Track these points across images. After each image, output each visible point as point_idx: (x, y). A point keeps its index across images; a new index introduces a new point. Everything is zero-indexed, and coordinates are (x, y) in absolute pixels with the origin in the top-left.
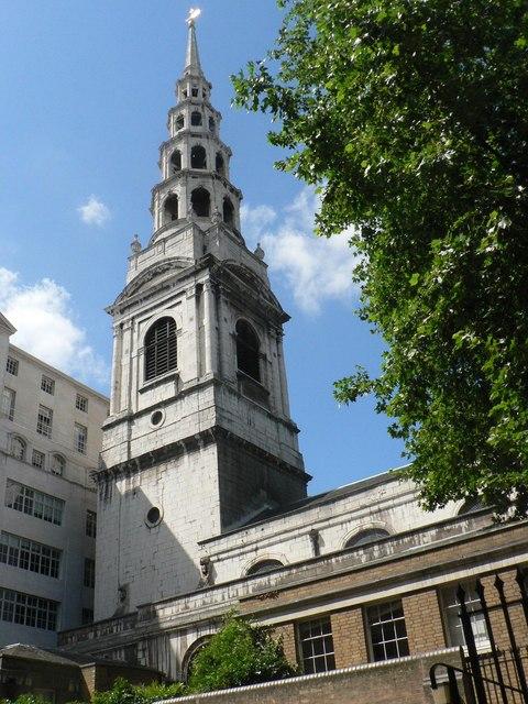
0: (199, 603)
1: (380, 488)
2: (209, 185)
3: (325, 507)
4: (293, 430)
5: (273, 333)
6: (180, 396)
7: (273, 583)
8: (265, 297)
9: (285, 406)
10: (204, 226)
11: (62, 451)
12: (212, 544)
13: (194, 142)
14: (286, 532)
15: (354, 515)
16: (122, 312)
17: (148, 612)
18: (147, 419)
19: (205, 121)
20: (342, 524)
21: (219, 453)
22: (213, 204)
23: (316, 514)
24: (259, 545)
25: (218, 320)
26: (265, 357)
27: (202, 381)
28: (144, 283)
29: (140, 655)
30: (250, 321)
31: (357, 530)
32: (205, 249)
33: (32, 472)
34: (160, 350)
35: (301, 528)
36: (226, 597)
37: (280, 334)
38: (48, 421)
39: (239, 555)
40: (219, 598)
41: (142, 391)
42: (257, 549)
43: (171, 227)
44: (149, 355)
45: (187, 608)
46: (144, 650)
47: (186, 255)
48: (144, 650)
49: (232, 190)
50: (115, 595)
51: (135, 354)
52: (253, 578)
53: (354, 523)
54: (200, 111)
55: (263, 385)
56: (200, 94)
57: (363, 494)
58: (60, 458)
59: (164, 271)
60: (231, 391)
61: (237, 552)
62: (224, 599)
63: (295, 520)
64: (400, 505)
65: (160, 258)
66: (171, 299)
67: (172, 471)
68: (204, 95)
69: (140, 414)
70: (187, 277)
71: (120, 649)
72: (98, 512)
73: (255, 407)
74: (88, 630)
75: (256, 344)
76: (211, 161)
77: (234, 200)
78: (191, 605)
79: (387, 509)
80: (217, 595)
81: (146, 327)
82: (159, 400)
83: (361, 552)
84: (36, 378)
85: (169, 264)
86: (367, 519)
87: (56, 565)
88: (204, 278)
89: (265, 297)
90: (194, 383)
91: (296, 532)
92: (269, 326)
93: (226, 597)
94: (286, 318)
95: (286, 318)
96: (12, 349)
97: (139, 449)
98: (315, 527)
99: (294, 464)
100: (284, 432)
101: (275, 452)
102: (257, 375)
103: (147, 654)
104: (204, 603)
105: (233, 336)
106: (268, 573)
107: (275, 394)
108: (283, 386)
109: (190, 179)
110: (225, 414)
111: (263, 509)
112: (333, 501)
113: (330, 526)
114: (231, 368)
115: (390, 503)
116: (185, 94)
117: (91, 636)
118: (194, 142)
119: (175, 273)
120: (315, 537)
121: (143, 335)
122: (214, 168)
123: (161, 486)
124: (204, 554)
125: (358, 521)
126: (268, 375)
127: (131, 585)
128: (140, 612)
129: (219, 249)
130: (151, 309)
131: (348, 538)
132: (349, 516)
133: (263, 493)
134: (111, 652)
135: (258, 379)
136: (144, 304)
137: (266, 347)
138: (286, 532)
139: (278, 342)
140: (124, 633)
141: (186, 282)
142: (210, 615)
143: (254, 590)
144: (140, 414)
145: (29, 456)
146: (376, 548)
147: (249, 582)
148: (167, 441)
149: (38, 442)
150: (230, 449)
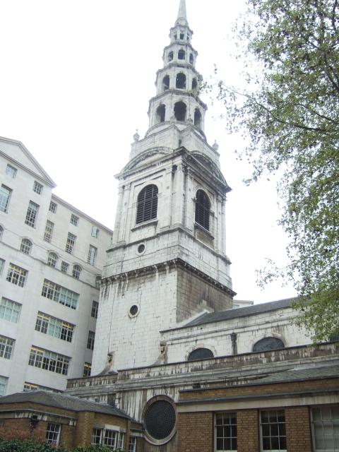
0: (157, 374)
1: (280, 312)
2: (186, 100)
3: (243, 319)
4: (227, 262)
5: (220, 198)
6: (157, 236)
7: (204, 367)
8: (217, 176)
9: (223, 246)
10: (181, 127)
11: (80, 263)
12: (168, 333)
13: (179, 70)
14: (216, 332)
16: (125, 178)
17: (125, 375)
18: (135, 248)
19: (187, 57)
20: (253, 331)
21: (178, 275)
22: (188, 113)
23: (236, 323)
24: (198, 338)
25: (185, 189)
26: (213, 215)
27: (172, 228)
28: (139, 161)
29: (117, 401)
30: (206, 191)
31: (262, 337)
32: (180, 142)
33: (61, 274)
34: (147, 205)
36: (174, 373)
37: (224, 200)
38: (73, 243)
39: (185, 342)
40: (169, 373)
41: (133, 230)
42: (196, 340)
43: (160, 125)
44: (140, 207)
45: (148, 375)
46: (119, 399)
47: (168, 146)
48: (119, 399)
49: (201, 104)
50: (106, 358)
51: (130, 206)
52: (192, 362)
53: (260, 331)
54: (184, 49)
55: (210, 232)
56: (185, 38)
57: (268, 314)
58: (77, 267)
59: (153, 155)
60: (190, 236)
61: (184, 340)
63: (223, 326)
65: (152, 146)
66: (156, 173)
67: (148, 284)
68: (188, 38)
69: (130, 245)
70: (167, 160)
71: (105, 395)
72: (100, 302)
73: (204, 247)
74: (86, 380)
75: (208, 205)
76: (189, 83)
77: (202, 110)
78: (151, 374)
80: (169, 370)
82: (143, 238)
83: (263, 355)
84: (68, 214)
85: (157, 151)
86: (269, 330)
87: (70, 334)
88: (178, 161)
89: (217, 176)
90: (167, 229)
91: (223, 333)
92: (218, 194)
93: (174, 373)
94: (229, 189)
95: (229, 189)
96: (53, 197)
97: (129, 267)
98: (236, 331)
99: (226, 284)
100: (221, 263)
101: (214, 276)
102: (207, 226)
103: (121, 401)
104: (160, 374)
105: (194, 200)
106: (202, 360)
107: (218, 239)
108: (223, 233)
109: (174, 95)
110: (185, 251)
111: (203, 313)
112: (249, 316)
113: (244, 332)
114: (191, 222)
116: (176, 37)
117: (88, 384)
118: (179, 70)
119: (161, 156)
120: (234, 337)
121: (137, 195)
122: (190, 88)
123: (140, 293)
124: (162, 339)
126: (214, 225)
128: (120, 374)
129: (191, 145)
130: (143, 178)
131: (256, 341)
132: (257, 328)
133: (205, 302)
134: (99, 396)
135: (208, 228)
136: (139, 174)
137: (214, 207)
138: (216, 332)
139: (223, 205)
140: (109, 386)
141: (167, 163)
142: (163, 383)
143: (192, 370)
144: (130, 245)
145: (59, 265)
146: (273, 354)
147: (190, 365)
148: (147, 264)
149: (64, 257)
150: (185, 273)
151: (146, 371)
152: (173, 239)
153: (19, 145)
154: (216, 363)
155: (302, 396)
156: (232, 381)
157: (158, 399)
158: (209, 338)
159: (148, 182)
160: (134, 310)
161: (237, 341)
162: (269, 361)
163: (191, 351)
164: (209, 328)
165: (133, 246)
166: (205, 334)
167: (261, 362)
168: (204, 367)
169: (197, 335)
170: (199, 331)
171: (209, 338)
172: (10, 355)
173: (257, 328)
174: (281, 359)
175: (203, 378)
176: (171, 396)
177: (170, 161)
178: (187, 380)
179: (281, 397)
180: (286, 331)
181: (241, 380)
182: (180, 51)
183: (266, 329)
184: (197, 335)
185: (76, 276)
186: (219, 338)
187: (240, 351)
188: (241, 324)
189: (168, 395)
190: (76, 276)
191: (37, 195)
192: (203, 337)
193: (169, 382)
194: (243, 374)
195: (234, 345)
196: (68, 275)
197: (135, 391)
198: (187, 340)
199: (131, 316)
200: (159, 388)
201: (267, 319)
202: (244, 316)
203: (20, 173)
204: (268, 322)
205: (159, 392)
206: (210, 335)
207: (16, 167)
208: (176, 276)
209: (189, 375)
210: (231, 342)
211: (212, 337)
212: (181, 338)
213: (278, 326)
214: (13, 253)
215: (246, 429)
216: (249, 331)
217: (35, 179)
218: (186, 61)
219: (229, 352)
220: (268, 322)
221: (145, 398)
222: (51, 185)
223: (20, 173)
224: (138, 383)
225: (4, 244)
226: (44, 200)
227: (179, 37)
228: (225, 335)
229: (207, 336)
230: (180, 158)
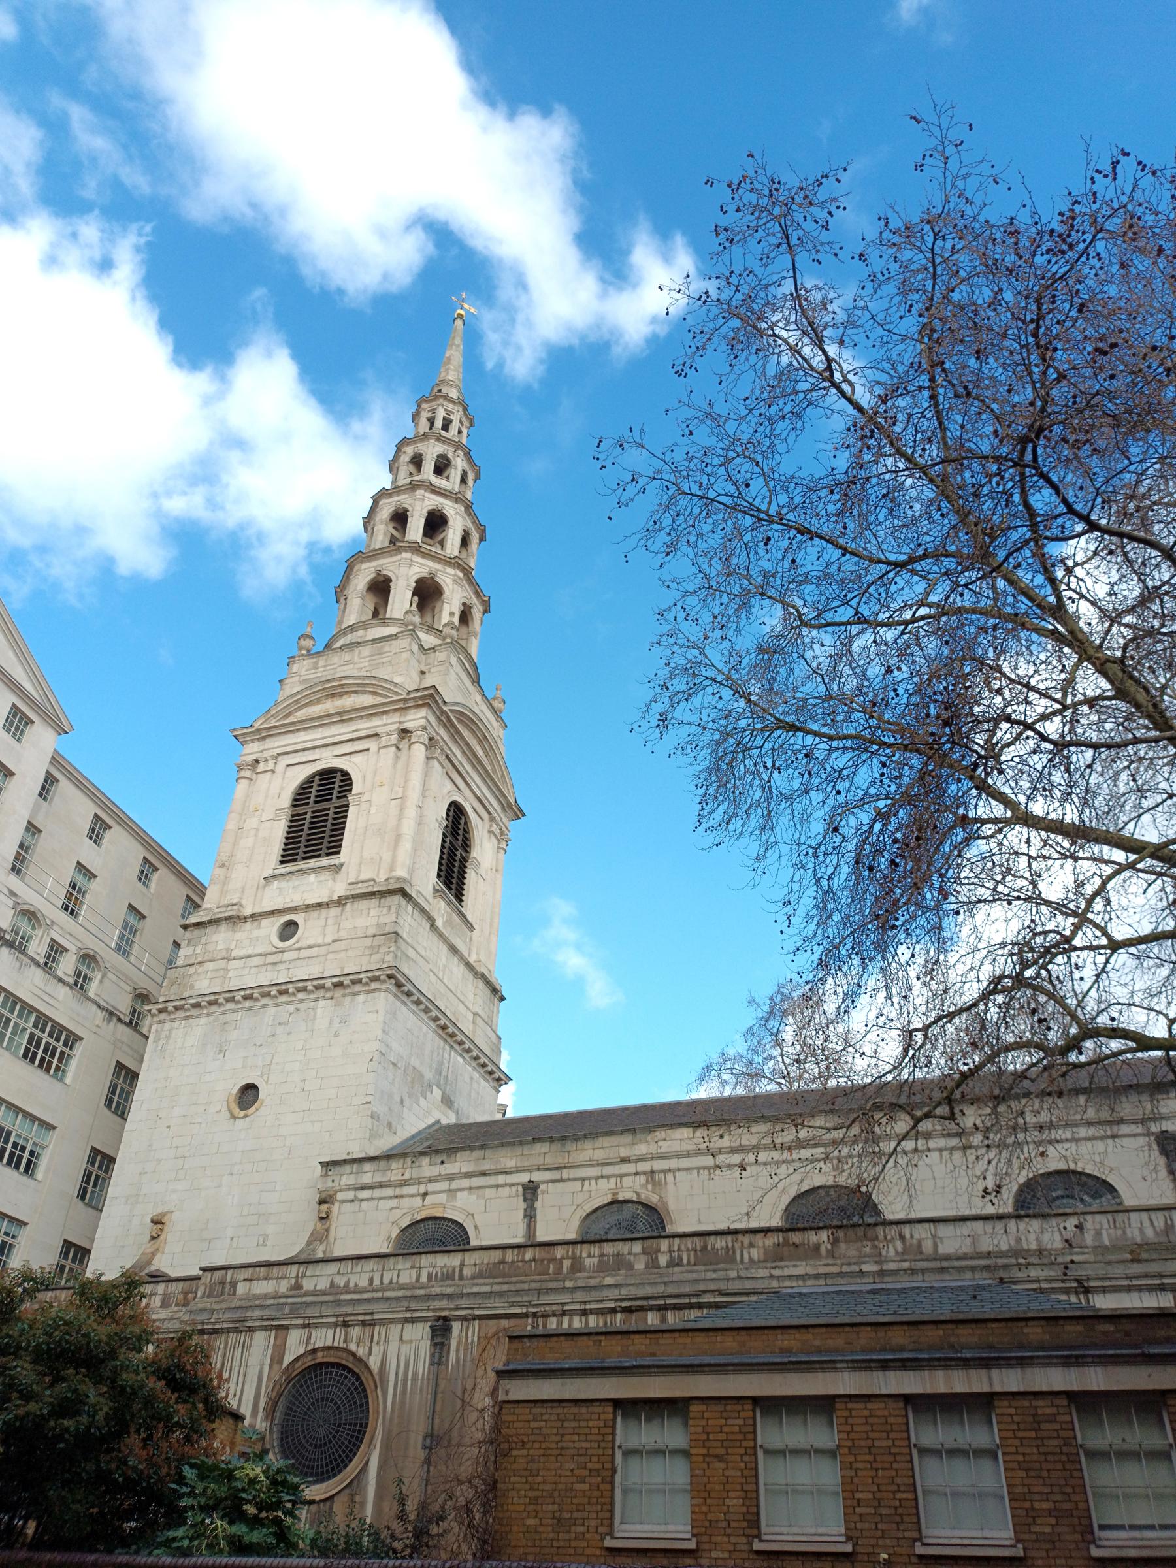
7: (467, 1272)
14: (484, 1174)
15: (608, 1170)
17: (223, 1283)
20: (583, 1180)
36: (376, 1282)
42: (426, 1194)
45: (297, 1287)
53: (602, 1182)
54: (450, 455)
61: (389, 1192)
62: (371, 1281)
63: (507, 1159)
78: (308, 1285)
81: (301, 774)
83: (637, 1247)
84: (85, 811)
86: (627, 1181)
91: (501, 1179)
93: (376, 1282)
98: (537, 1177)
113: (561, 1180)
115: (673, 1164)
118: (433, 501)
120: (531, 1191)
127: (174, 1217)
132: (595, 1171)
141: (385, 719)
142: (338, 1311)
147: (426, 1260)
151: (293, 1271)
152: (368, 916)
154: (503, 1262)
155: (885, 1365)
156: (545, 1316)
157: (320, 1358)
159: (328, 759)
160: (249, 1094)
161: (538, 1205)
162: (653, 1264)
163: (405, 1222)
164: (463, 1163)
165: (265, 922)
166: (451, 1177)
167: (630, 1267)
168: (467, 1272)
169: (430, 1180)
170: (435, 1170)
174: (685, 1261)
175: (464, 1303)
176: (361, 1352)
177: (396, 717)
178: (413, 1305)
179: (828, 1366)
180: (670, 1187)
181: (572, 1313)
182: (438, 456)
183: (621, 1176)
184: (430, 1180)
185: (80, 983)
186: (489, 1193)
187: (542, 1236)
188: (549, 1160)
189: (353, 1347)
190: (80, 983)
191: (14, 742)
192: (444, 1185)
193: (360, 1309)
194: (579, 1296)
195: (530, 1216)
196: (60, 980)
197: (251, 1330)
198: (398, 1191)
199: (237, 1111)
200: (327, 1325)
201: (624, 1152)
204: (625, 1160)
205: (323, 1338)
206: (465, 1183)
208: (382, 1012)
209: (422, 1292)
210: (522, 1205)
212: (381, 1186)
213: (652, 1172)
215: (720, 1458)
217: (11, 699)
218: (451, 482)
220: (625, 1160)
221: (277, 1357)
224: (263, 1307)
227: (439, 423)
228: (506, 1185)
229: (455, 1184)
230: (423, 712)
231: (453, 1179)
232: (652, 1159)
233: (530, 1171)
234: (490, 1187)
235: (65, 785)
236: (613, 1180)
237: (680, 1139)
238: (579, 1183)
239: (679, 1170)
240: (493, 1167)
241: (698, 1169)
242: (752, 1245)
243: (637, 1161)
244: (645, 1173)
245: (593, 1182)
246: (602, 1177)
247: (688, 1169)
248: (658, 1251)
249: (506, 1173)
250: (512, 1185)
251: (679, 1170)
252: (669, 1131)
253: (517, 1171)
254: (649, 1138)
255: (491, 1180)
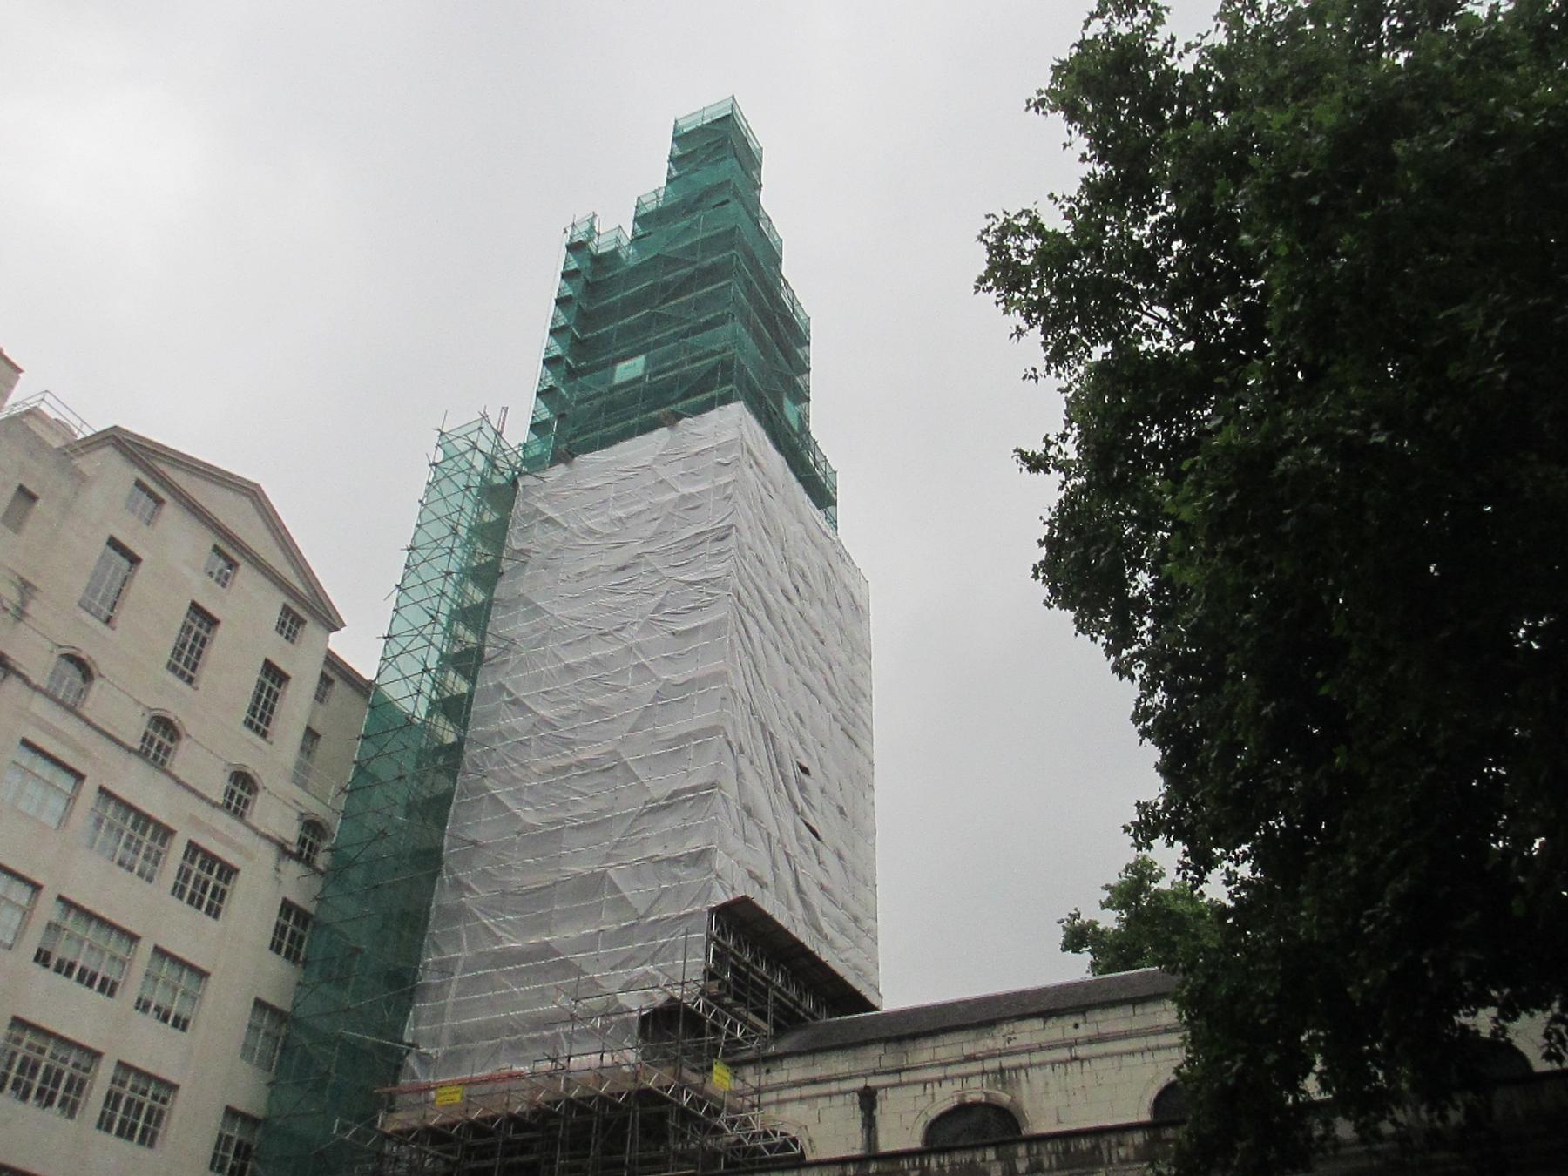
1: (1006, 1028)
14: (814, 1082)
15: (950, 1071)
20: (925, 1083)
23: (876, 1056)
31: (952, 1103)
35: (845, 1079)
53: (947, 1085)
63: (837, 1064)
64: (1041, 1065)
79: (1016, 1069)
83: (991, 1154)
86: (975, 1082)
91: (834, 1087)
96: (332, 661)
98: (873, 1082)
112: (914, 1037)
113: (901, 1084)
115: (1024, 1059)
120: (868, 1099)
125: (958, 1085)
131: (933, 1113)
132: (937, 1073)
138: (814, 1082)
153: (253, 493)
158: (791, 1100)
161: (876, 1113)
166: (779, 1088)
171: (791, 1100)
172: (154, 1135)
173: (937, 1073)
180: (1024, 1085)
183: (966, 1076)
187: (886, 1144)
188: (889, 1062)
195: (869, 1124)
201: (969, 1049)
202: (899, 1039)
203: (246, 575)
204: (971, 1058)
206: (796, 1092)
207: (235, 556)
210: (859, 1114)
211: (801, 1099)
213: (1002, 1070)
214: (201, 810)
216: (916, 1083)
217: (281, 599)
219: (854, 1146)
220: (971, 1058)
222: (332, 622)
223: (246, 575)
225: (179, 782)
226: (303, 669)
229: (785, 1095)
231: (781, 1089)
232: (1000, 1055)
233: (865, 1076)
234: (826, 1095)
235: (339, 685)
236: (958, 1083)
237: (1029, 1032)
238: (921, 1087)
239: (1031, 1066)
240: (824, 1073)
241: (1053, 1063)
242: (1120, 1144)
243: (982, 1059)
244: (993, 1072)
245: (936, 1084)
246: (946, 1078)
247: (1041, 1065)
248: (1016, 1155)
249: (839, 1080)
250: (845, 1093)
251: (1031, 1066)
252: (1016, 1023)
253: (849, 1077)
254: (995, 1031)
255: (823, 1089)
